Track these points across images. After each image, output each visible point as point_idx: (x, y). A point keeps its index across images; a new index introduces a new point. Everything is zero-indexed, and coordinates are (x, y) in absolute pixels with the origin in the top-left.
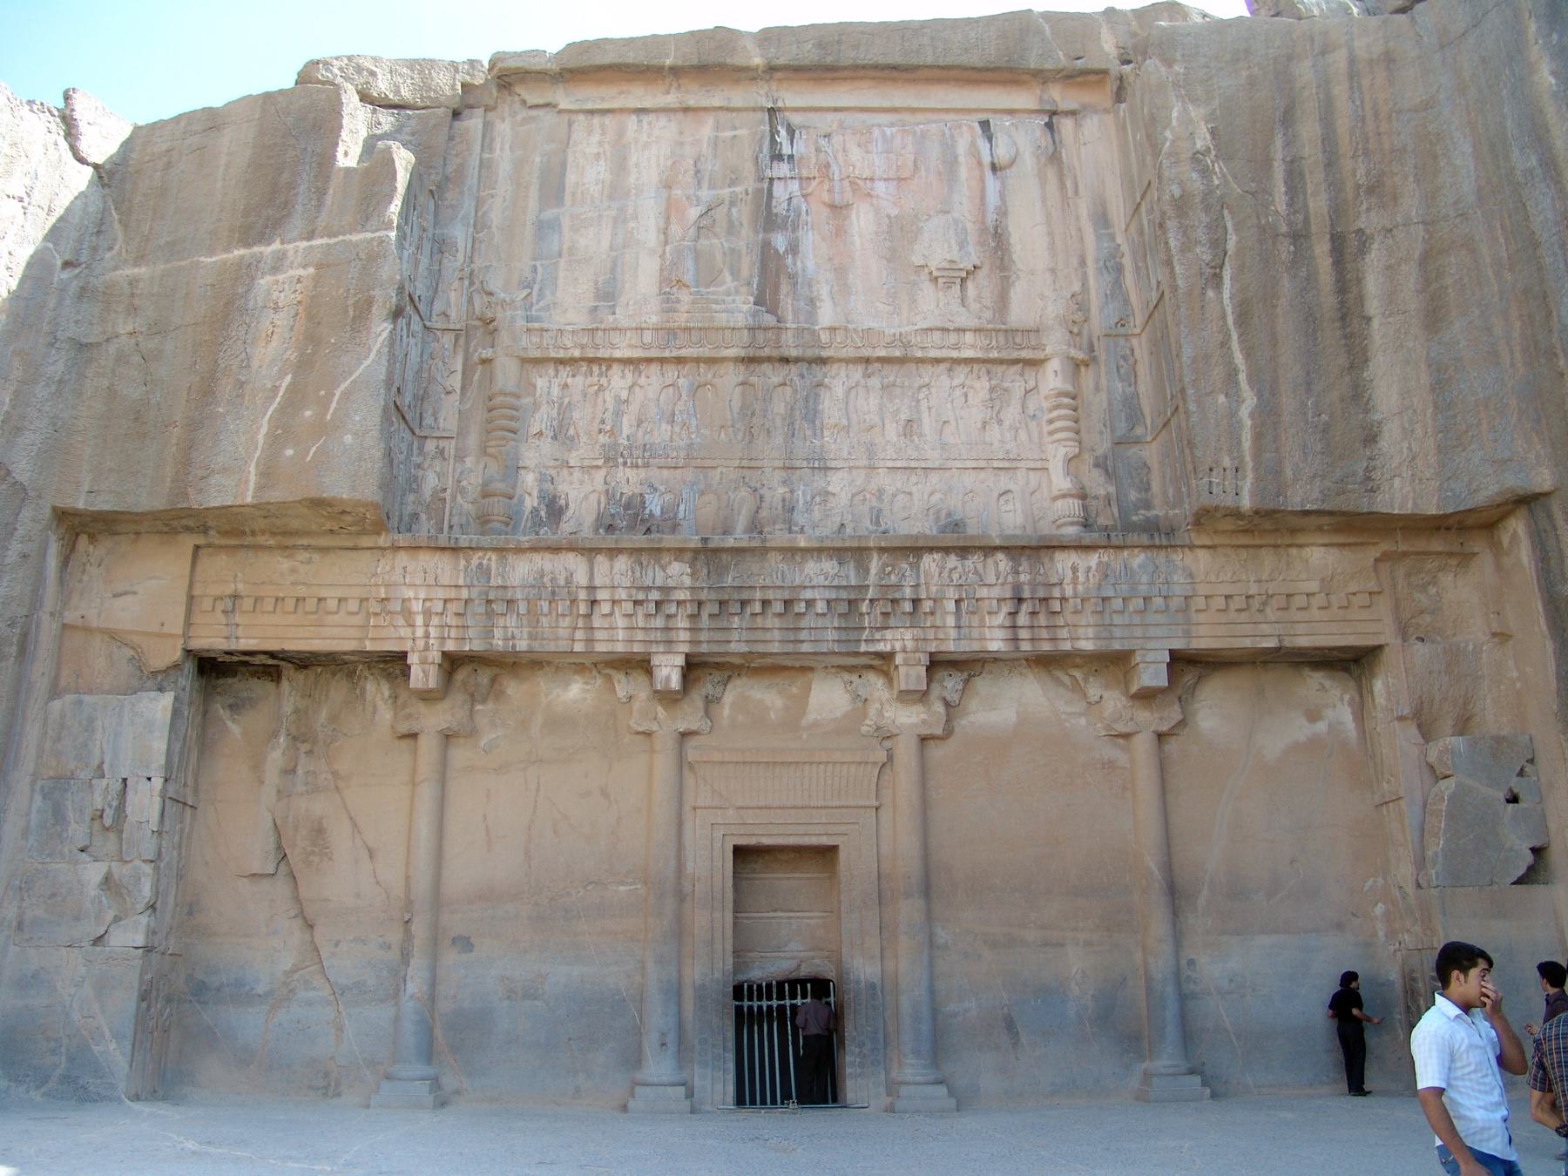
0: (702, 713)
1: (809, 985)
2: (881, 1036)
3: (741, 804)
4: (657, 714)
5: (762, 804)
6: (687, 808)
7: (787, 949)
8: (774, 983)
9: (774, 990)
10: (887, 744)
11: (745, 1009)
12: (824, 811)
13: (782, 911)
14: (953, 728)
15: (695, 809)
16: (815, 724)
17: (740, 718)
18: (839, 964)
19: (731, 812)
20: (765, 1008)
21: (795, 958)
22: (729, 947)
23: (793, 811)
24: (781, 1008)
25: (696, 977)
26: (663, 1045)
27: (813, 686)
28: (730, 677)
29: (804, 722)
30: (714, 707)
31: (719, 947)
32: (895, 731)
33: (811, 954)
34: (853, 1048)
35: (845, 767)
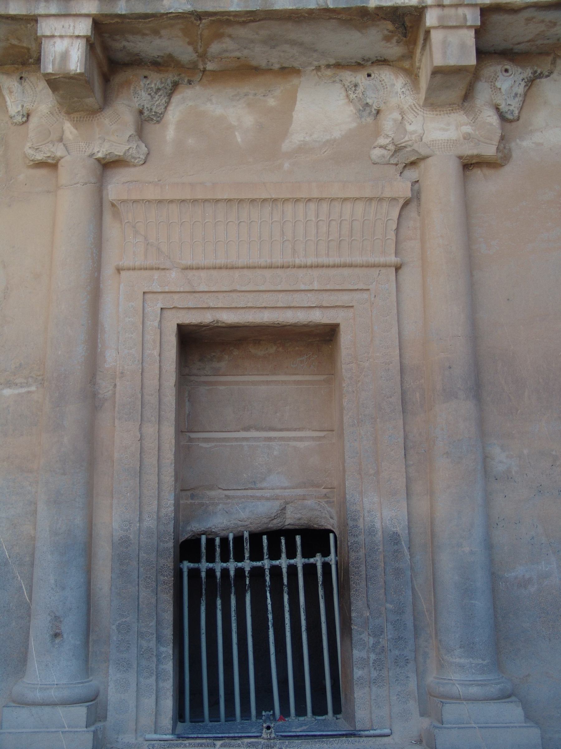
0: (131, 131)
1: (298, 539)
2: (408, 618)
3: (189, 262)
4: (63, 132)
5: (221, 261)
6: (108, 271)
7: (264, 485)
8: (246, 535)
9: (247, 546)
10: (412, 174)
11: (203, 575)
12: (316, 273)
13: (257, 429)
14: (510, 150)
15: (119, 270)
16: (303, 149)
17: (191, 141)
18: (343, 504)
19: (173, 274)
20: (232, 573)
21: (276, 498)
22: (168, 478)
23: (268, 273)
24: (258, 573)
25: (115, 525)
26: (56, 635)
27: (300, 96)
28: (175, 85)
29: (286, 146)
30: (151, 129)
31: (151, 478)
32: (423, 151)
33: (300, 492)
34: (364, 636)
35: (348, 207)
